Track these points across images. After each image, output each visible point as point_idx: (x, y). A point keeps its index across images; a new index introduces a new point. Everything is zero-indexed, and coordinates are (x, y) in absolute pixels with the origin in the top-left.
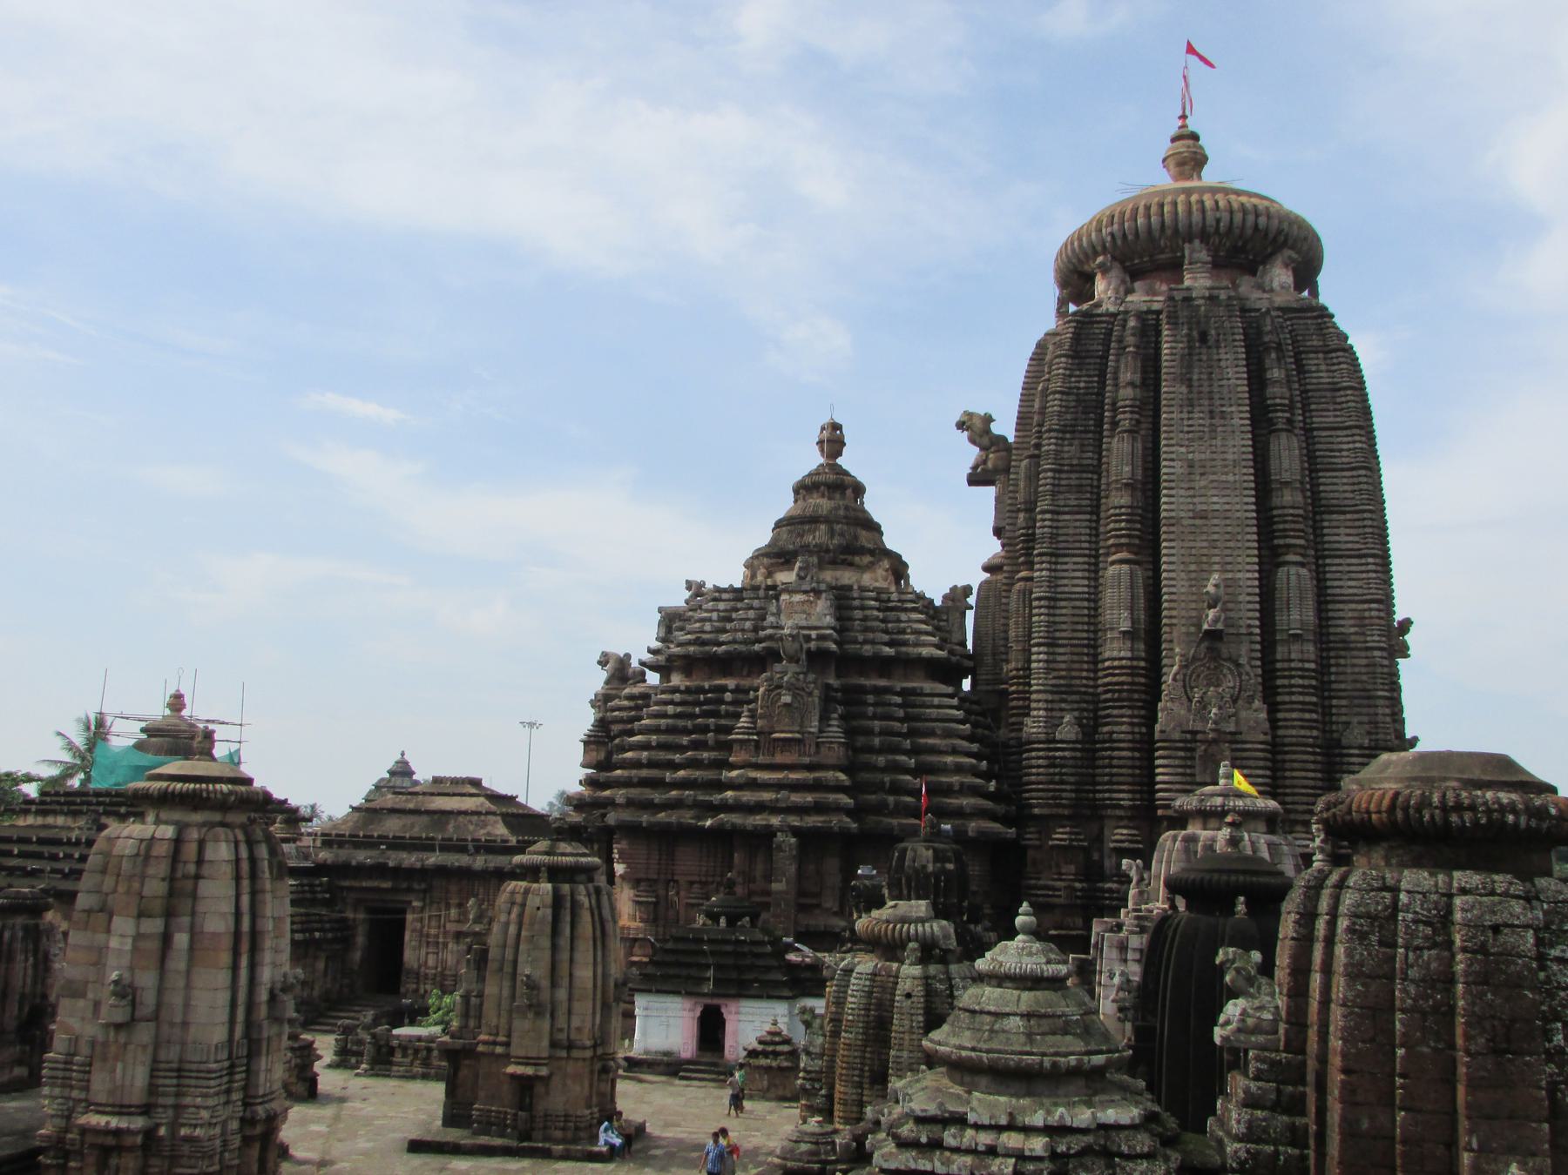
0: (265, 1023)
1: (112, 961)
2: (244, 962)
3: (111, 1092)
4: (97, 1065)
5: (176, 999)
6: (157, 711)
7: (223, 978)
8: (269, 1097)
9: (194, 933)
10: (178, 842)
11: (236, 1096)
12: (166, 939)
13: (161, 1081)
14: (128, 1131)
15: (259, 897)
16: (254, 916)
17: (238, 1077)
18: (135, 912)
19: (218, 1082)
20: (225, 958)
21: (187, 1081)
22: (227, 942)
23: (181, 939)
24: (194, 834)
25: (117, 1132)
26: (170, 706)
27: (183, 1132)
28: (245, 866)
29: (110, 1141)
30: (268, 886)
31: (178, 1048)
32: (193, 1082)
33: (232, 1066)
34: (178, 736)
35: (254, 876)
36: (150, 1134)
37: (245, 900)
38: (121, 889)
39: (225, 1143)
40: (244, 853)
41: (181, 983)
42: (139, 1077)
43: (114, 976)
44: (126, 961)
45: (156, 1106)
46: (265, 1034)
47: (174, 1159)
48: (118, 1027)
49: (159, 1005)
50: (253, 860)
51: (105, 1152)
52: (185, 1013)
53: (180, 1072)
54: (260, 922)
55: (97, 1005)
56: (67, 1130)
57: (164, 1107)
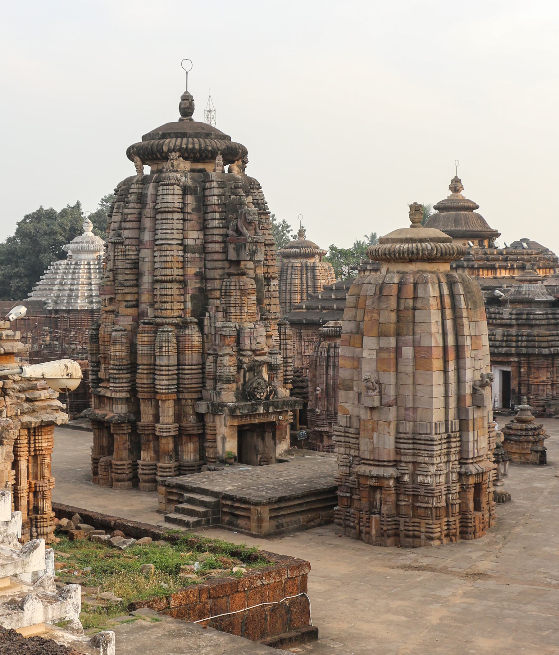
0: (471, 409)
1: (365, 366)
2: (452, 366)
3: (372, 452)
4: (362, 433)
5: (408, 392)
6: (446, 194)
7: (437, 378)
8: (477, 459)
9: (416, 347)
10: (400, 285)
11: (453, 458)
12: (398, 350)
13: (402, 446)
14: (384, 478)
15: (459, 321)
16: (458, 333)
17: (453, 445)
18: (375, 332)
19: (439, 447)
20: (437, 364)
21: (418, 446)
22: (437, 353)
23: (408, 352)
24: (412, 280)
25: (378, 478)
26: (450, 189)
27: (420, 479)
28: (447, 300)
29: (373, 482)
30: (465, 314)
31: (411, 423)
32: (422, 447)
33: (449, 437)
34: (457, 210)
35: (454, 307)
36: (398, 480)
37: (449, 323)
38: (366, 319)
39: (448, 489)
40: (446, 291)
41: (410, 381)
42: (387, 443)
43: (365, 375)
44: (373, 366)
45: (401, 461)
46: (471, 417)
47: (415, 496)
48: (372, 409)
49: (397, 396)
50: (453, 296)
51: (374, 489)
52: (414, 401)
53: (414, 440)
54: (460, 338)
55: (360, 395)
56: (350, 474)
57: (406, 462)
